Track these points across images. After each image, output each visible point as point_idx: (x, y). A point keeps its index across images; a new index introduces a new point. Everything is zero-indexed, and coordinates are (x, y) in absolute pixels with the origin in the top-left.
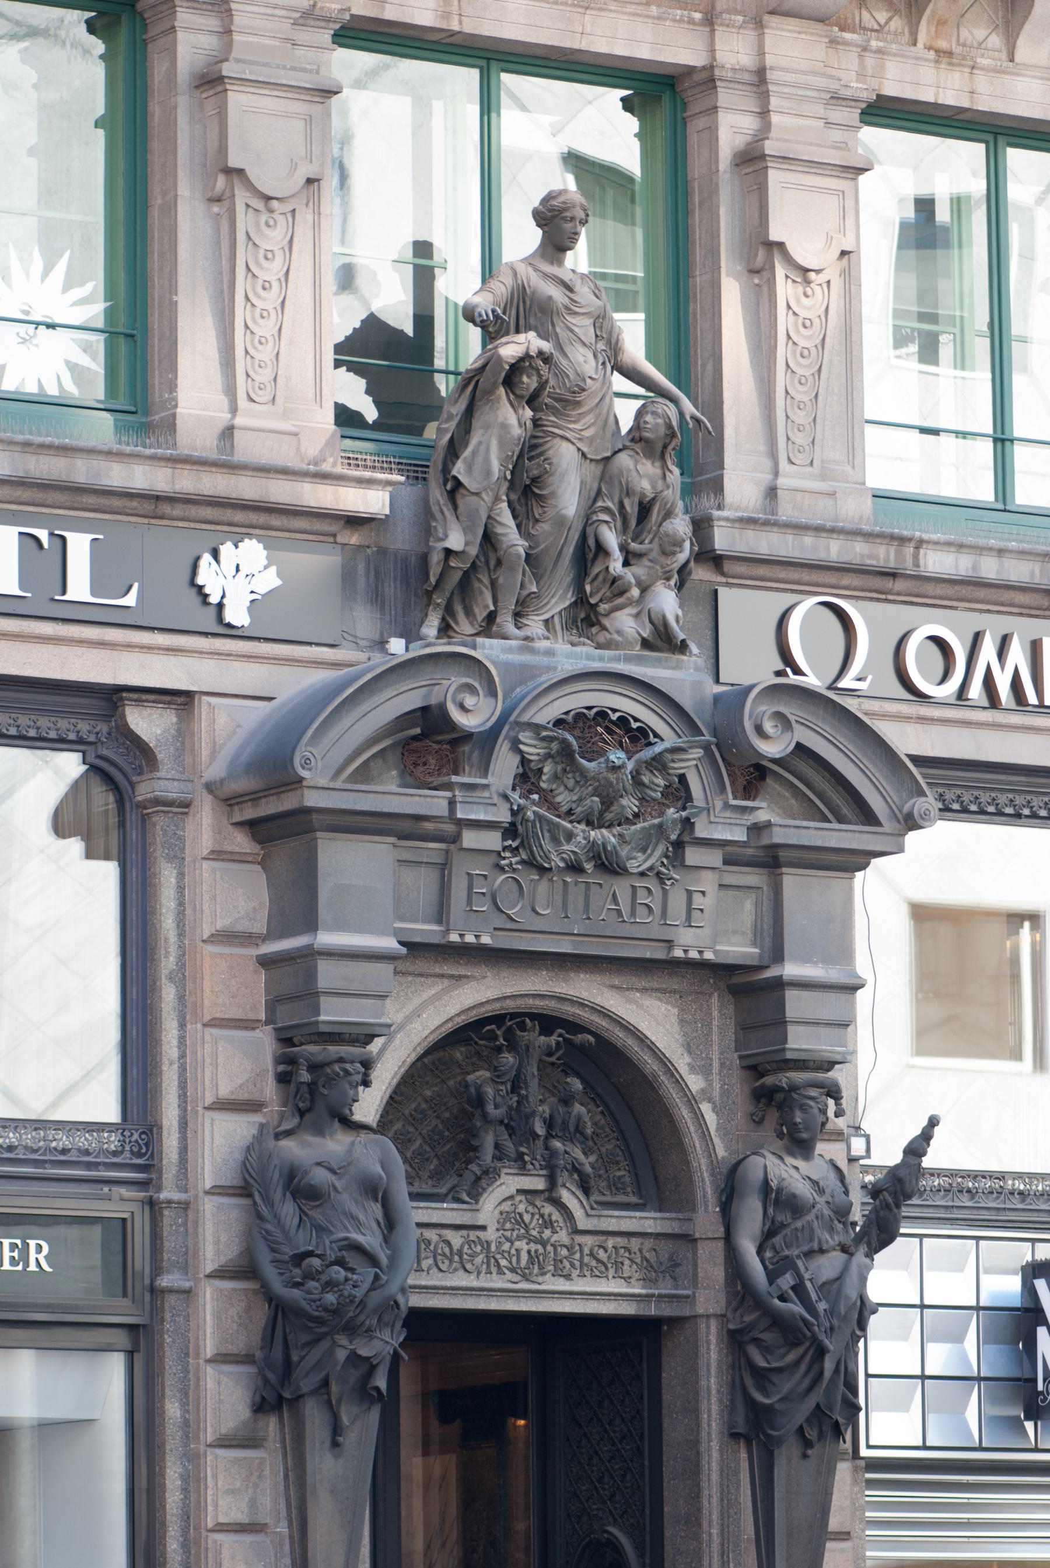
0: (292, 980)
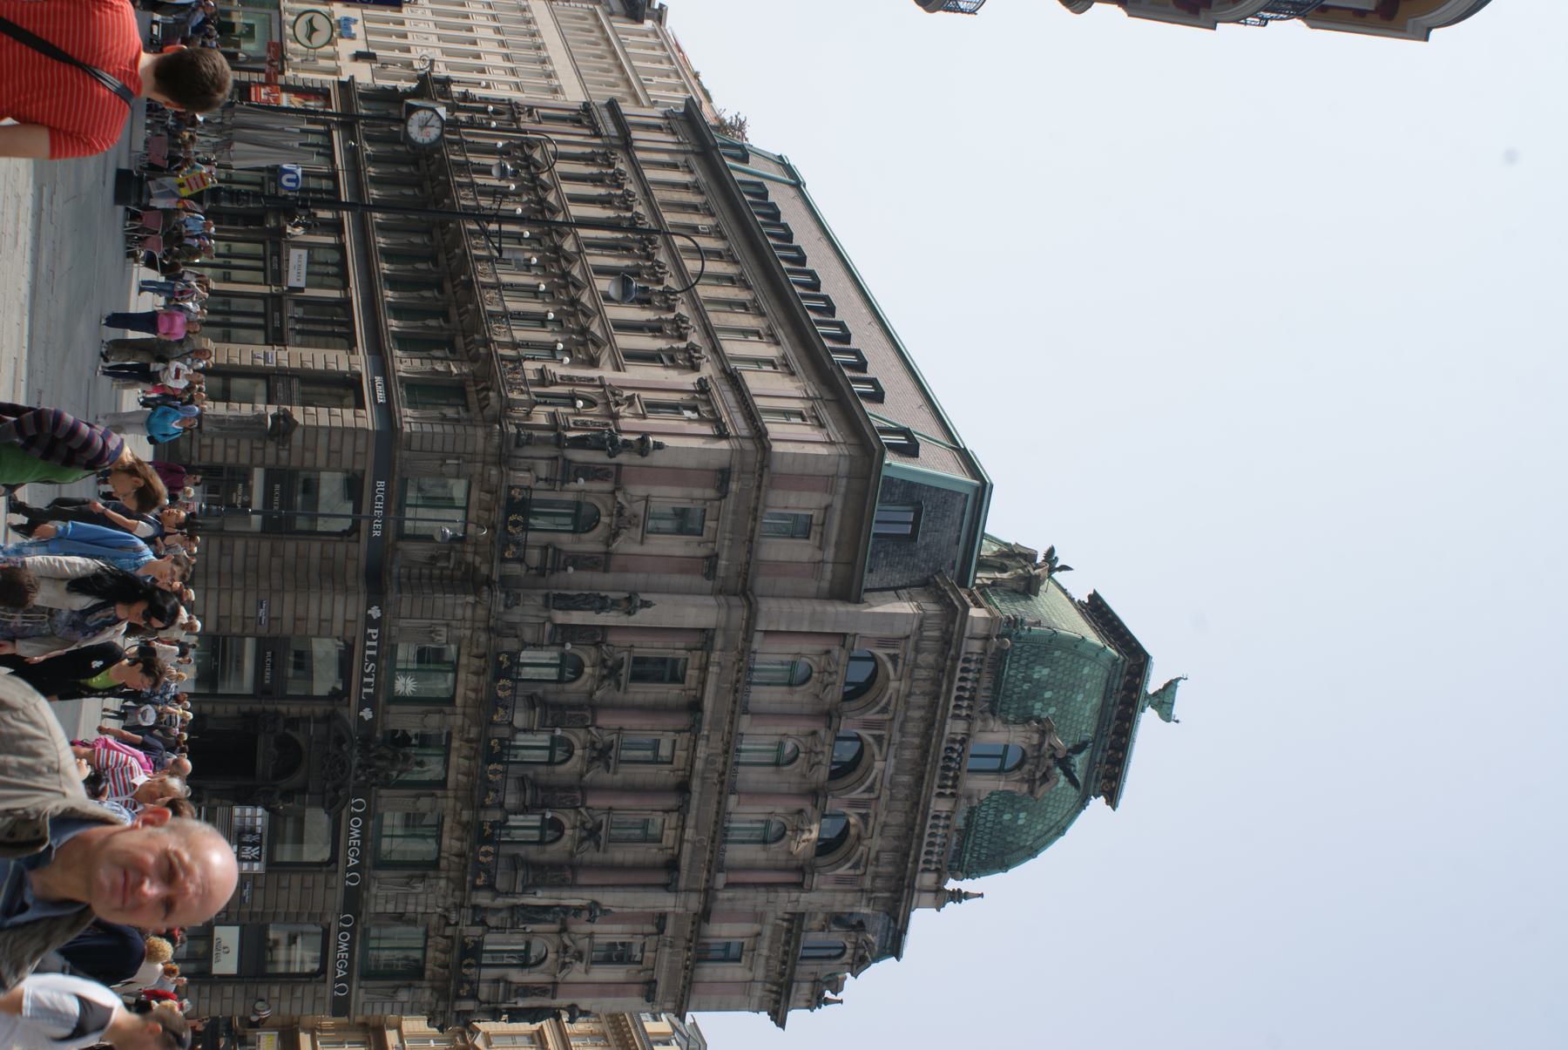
0: (306, 720)
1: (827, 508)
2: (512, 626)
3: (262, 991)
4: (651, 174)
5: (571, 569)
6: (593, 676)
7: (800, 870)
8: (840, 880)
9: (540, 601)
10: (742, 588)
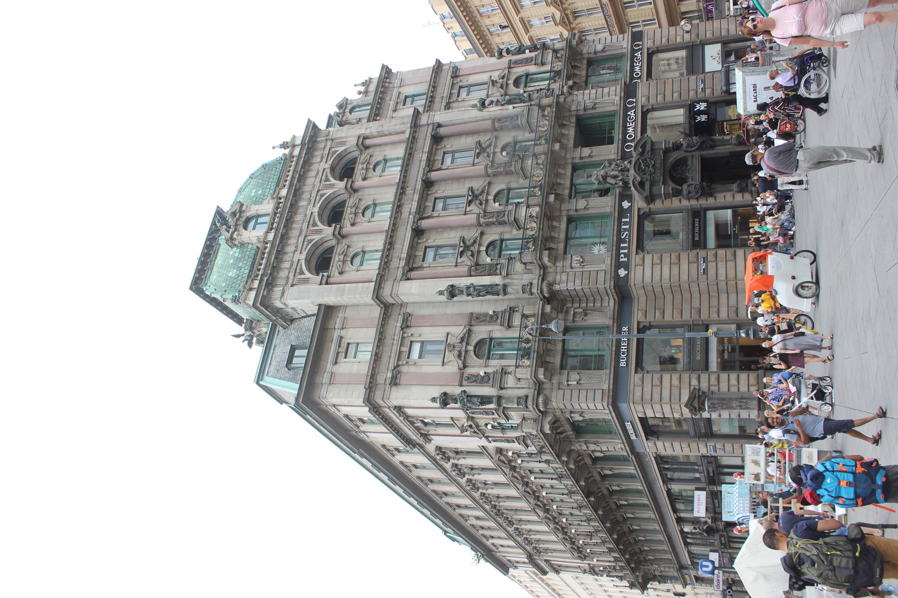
0: (667, 196)
1: (336, 363)
2: (529, 271)
3: (687, 37)
4: (511, 543)
5: (491, 313)
6: (480, 245)
7: (367, 148)
8: (343, 143)
9: (509, 290)
10: (387, 308)
